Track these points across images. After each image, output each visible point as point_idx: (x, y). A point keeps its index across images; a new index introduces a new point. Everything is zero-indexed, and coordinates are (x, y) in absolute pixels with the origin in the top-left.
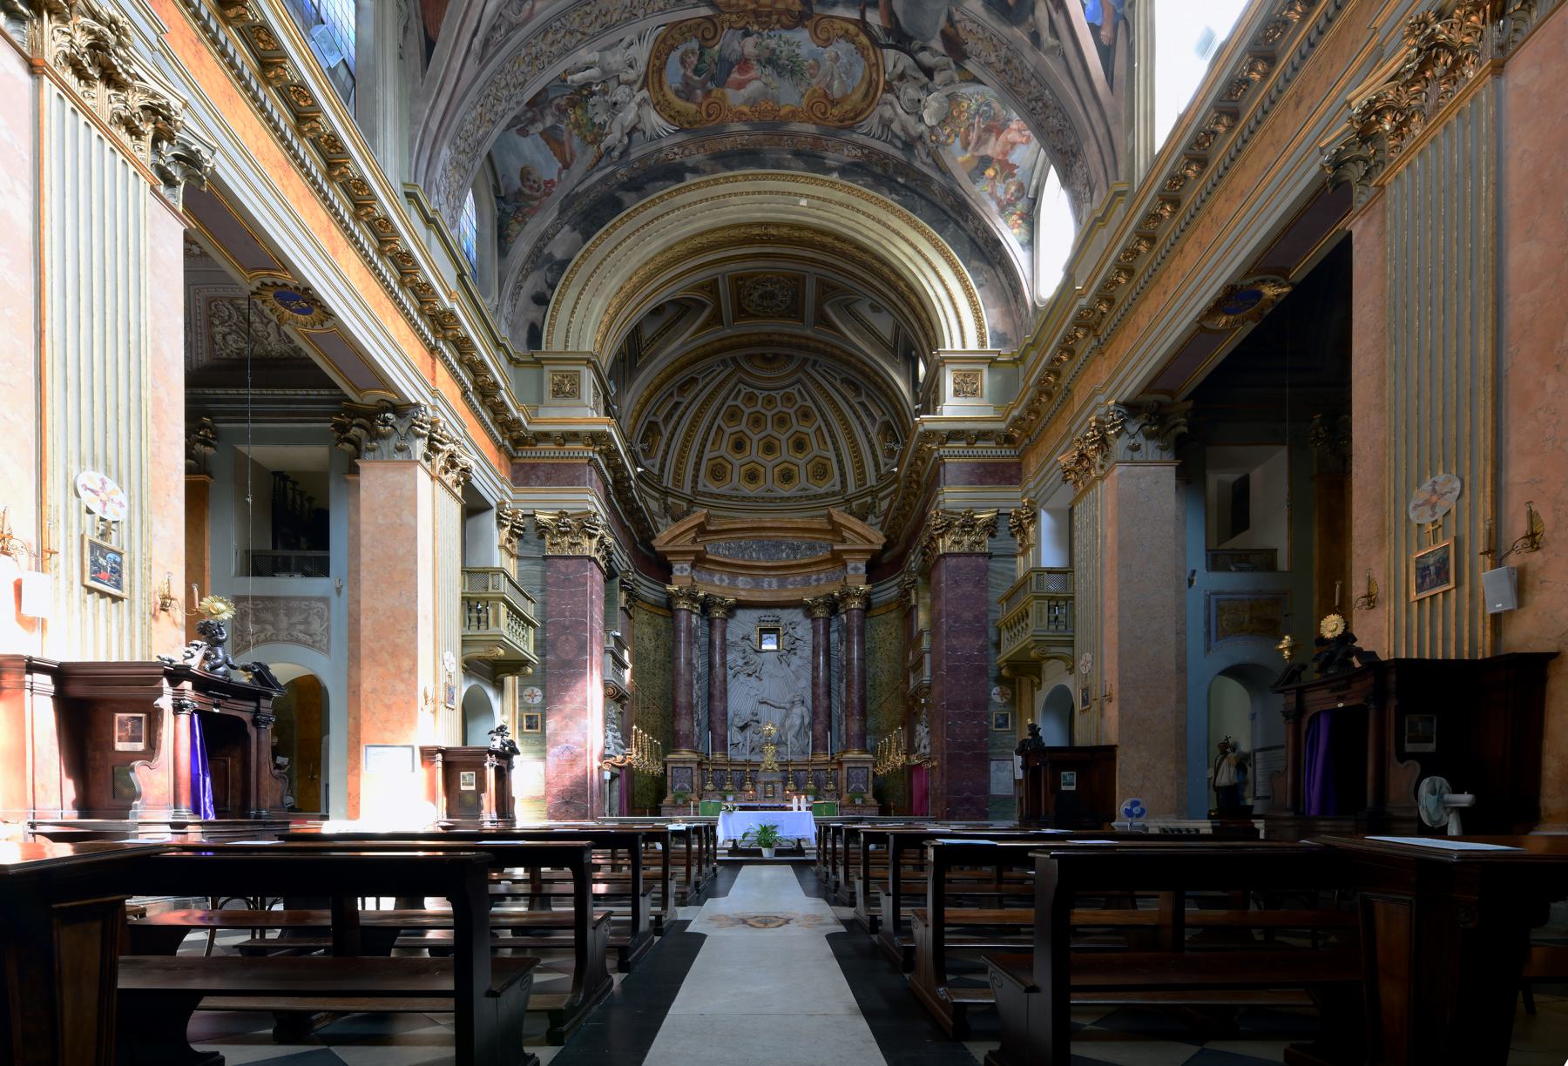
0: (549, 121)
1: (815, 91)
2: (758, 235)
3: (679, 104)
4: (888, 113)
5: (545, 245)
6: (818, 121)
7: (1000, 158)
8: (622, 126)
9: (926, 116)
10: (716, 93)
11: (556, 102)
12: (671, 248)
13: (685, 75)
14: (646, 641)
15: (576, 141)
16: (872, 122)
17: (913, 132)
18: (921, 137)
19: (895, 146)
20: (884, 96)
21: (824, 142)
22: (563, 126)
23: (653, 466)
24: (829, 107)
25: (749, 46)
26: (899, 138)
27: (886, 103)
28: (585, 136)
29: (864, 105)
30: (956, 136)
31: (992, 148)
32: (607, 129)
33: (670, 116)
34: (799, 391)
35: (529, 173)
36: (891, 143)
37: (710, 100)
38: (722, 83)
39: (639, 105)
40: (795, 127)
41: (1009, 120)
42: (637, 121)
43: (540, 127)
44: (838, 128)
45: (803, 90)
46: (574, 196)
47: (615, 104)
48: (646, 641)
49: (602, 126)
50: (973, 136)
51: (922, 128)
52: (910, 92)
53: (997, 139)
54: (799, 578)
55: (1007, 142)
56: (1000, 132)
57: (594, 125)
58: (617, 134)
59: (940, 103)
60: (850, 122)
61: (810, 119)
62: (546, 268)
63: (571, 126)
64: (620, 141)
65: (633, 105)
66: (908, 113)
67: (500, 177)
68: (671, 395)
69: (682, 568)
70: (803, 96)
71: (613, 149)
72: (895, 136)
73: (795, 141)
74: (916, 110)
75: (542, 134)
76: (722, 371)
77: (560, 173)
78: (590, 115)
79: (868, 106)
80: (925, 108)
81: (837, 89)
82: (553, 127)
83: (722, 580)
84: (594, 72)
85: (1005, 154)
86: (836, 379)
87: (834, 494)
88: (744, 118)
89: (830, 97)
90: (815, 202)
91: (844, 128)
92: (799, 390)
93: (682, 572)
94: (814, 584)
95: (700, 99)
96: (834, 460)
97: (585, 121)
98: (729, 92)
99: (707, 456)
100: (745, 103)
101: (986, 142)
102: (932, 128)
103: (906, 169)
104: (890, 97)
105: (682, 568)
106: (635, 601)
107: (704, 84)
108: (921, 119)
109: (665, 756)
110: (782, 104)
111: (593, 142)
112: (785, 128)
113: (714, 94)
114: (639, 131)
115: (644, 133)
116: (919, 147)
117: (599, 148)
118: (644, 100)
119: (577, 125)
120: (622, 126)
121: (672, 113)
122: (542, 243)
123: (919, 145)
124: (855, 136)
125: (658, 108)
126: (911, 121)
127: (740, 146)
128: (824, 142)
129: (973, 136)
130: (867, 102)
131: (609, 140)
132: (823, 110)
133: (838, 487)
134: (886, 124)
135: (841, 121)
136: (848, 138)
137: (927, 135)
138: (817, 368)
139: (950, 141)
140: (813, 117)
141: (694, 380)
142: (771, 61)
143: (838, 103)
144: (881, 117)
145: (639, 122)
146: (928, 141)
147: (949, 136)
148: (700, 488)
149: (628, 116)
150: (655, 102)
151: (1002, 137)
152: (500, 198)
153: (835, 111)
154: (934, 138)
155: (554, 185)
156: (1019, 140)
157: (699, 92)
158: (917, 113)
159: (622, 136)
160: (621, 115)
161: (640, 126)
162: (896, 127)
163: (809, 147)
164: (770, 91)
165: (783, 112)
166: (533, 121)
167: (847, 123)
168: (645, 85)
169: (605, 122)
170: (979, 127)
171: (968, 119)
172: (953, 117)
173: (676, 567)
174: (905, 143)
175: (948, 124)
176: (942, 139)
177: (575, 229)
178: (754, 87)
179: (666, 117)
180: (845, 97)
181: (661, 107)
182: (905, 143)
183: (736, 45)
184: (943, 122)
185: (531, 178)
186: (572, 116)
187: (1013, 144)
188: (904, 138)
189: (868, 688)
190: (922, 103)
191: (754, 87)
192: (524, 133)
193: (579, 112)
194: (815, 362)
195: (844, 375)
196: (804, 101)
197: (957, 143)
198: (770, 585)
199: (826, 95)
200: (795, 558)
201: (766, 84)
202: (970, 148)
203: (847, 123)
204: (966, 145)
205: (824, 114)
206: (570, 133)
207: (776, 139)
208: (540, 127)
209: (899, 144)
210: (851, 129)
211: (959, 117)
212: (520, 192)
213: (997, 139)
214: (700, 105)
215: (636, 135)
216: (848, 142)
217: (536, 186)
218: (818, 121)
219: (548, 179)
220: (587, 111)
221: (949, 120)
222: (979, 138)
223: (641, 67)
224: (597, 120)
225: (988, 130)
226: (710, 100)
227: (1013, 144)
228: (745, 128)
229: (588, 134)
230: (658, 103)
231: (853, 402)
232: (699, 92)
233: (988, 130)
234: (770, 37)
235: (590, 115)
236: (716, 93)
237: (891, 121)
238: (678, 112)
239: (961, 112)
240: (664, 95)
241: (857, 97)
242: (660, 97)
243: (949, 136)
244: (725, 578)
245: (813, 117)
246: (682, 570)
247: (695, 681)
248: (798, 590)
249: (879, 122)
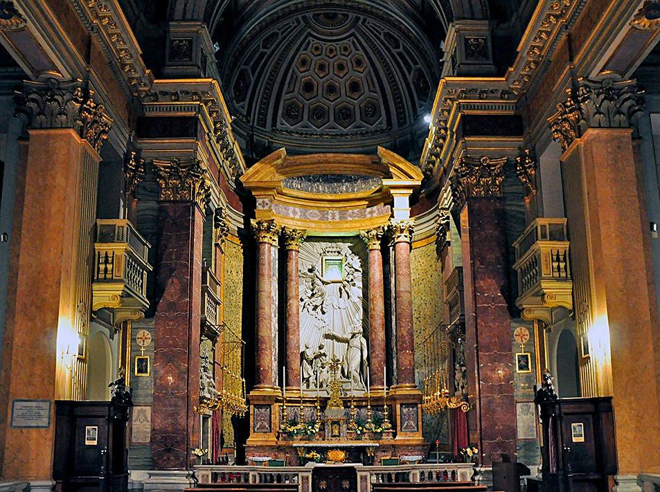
14: (234, 274)
23: (243, 108)
34: (353, 43)
48: (234, 274)
54: (356, 211)
68: (258, 47)
69: (263, 202)
76: (295, 27)
83: (294, 212)
86: (380, 33)
87: (382, 131)
92: (353, 43)
93: (263, 207)
94: (369, 216)
96: (381, 100)
99: (284, 96)
105: (263, 202)
106: (226, 235)
109: (248, 393)
133: (384, 126)
138: (366, 23)
141: (274, 35)
148: (279, 126)
173: (259, 201)
189: (414, 320)
194: (365, 20)
195: (386, 31)
198: (333, 218)
200: (353, 191)
231: (394, 51)
244: (297, 210)
246: (264, 204)
247: (273, 315)
248: (356, 221)
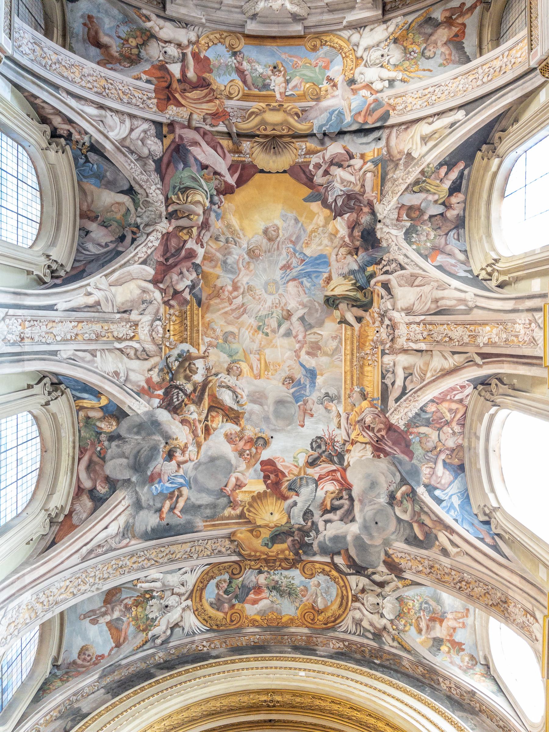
0: (116, 614)
1: (305, 605)
2: (265, 701)
3: (212, 612)
4: (358, 615)
5: (77, 700)
6: (310, 625)
7: (448, 638)
8: (168, 622)
9: (385, 612)
10: (238, 606)
11: (125, 602)
12: (188, 708)
13: (218, 594)
15: (132, 629)
16: (348, 623)
17: (378, 626)
18: (385, 628)
19: (368, 638)
20: (354, 604)
21: (315, 639)
22: (125, 619)
24: (316, 615)
25: (262, 579)
26: (369, 631)
27: (355, 609)
28: (139, 626)
29: (340, 612)
30: (411, 625)
31: (439, 632)
32: (157, 622)
33: (204, 619)
35: (87, 650)
36: (364, 636)
37: (233, 611)
38: (242, 601)
39: (184, 610)
40: (293, 630)
41: (445, 613)
42: (179, 620)
43: (108, 618)
44: (323, 629)
45: (297, 605)
46: (116, 667)
47: (167, 606)
49: (153, 620)
50: (423, 625)
51: (384, 622)
52: (370, 599)
53: (441, 626)
55: (448, 628)
56: (441, 621)
57: (148, 619)
58: (163, 627)
59: (393, 604)
60: (332, 624)
61: (304, 624)
62: (69, 719)
63: (131, 619)
64: (164, 633)
65: (179, 609)
66: (372, 613)
67: (63, 650)
70: (297, 609)
71: (157, 638)
72: (366, 630)
73: (293, 639)
74: (377, 609)
75: (107, 623)
77: (112, 649)
78: (147, 612)
79: (344, 612)
80: (383, 608)
81: (320, 604)
82: (118, 619)
84: (158, 585)
85: (451, 636)
88: (257, 624)
89: (316, 608)
90: (312, 674)
91: (328, 629)
95: (226, 610)
97: (142, 616)
98: (247, 606)
100: (258, 613)
101: (434, 628)
102: (392, 621)
103: (378, 653)
104: (357, 604)
107: (230, 600)
108: (382, 616)
110: (283, 614)
111: (144, 630)
112: (286, 630)
113: (236, 607)
114: (180, 627)
115: (183, 629)
116: (385, 635)
117: (147, 635)
118: (188, 607)
119: (136, 619)
120: (168, 622)
121: (206, 618)
122: (75, 698)
123: (385, 634)
124: (337, 633)
125: (196, 613)
126: (375, 618)
127: (252, 643)
128: (315, 639)
129: (423, 625)
130: (342, 610)
131: (155, 631)
132: (312, 618)
134: (358, 623)
135: (325, 624)
136: (332, 634)
137: (389, 626)
139: (407, 629)
140: (306, 623)
142: (275, 588)
143: (322, 612)
144: (353, 618)
145: (181, 621)
146: (391, 630)
147: (405, 625)
149: (174, 616)
150: (195, 609)
151: (444, 624)
152: (55, 666)
153: (321, 618)
154: (394, 627)
155: (102, 659)
156: (457, 625)
157: (226, 605)
158: (378, 612)
159: (167, 629)
160: (169, 614)
161: (181, 624)
162: (365, 624)
163: (304, 643)
164: (275, 606)
165: (284, 620)
166: (105, 614)
167: (329, 625)
168: (190, 597)
169: (156, 618)
170: (425, 618)
171: (415, 613)
172: (405, 613)
174: (374, 634)
175: (402, 618)
176: (401, 627)
177: (108, 693)
178: (264, 604)
179: (201, 620)
180: (326, 608)
181: (198, 612)
182: (374, 634)
183: (253, 578)
184: (399, 616)
185: (87, 653)
186: (134, 613)
187: (454, 629)
188: (373, 631)
190: (381, 604)
191: (264, 604)
192: (94, 622)
193: (140, 609)
196: (299, 613)
197: (413, 631)
199: (313, 607)
201: (272, 602)
202: (424, 632)
203: (329, 625)
204: (420, 631)
205: (313, 620)
206: (129, 624)
207: (279, 637)
208: (108, 618)
209: (370, 636)
210: (333, 629)
211: (409, 612)
212: (74, 662)
213: (441, 626)
214: (226, 614)
215: (177, 630)
216: (333, 638)
217: (89, 658)
218: (310, 625)
219: (100, 654)
220: (145, 610)
221: (402, 615)
222: (428, 626)
223: (190, 586)
224: (151, 616)
225: (432, 619)
226: (233, 611)
227: (454, 629)
228: (257, 630)
229: (141, 625)
230: (197, 610)
232: (226, 605)
233: (432, 619)
234: (275, 574)
235: (147, 612)
236: (238, 606)
237: (361, 620)
238: (210, 617)
239: (409, 609)
240: (202, 605)
241: (335, 607)
242: (199, 606)
243: (405, 625)
245: (306, 623)
249: (353, 622)
